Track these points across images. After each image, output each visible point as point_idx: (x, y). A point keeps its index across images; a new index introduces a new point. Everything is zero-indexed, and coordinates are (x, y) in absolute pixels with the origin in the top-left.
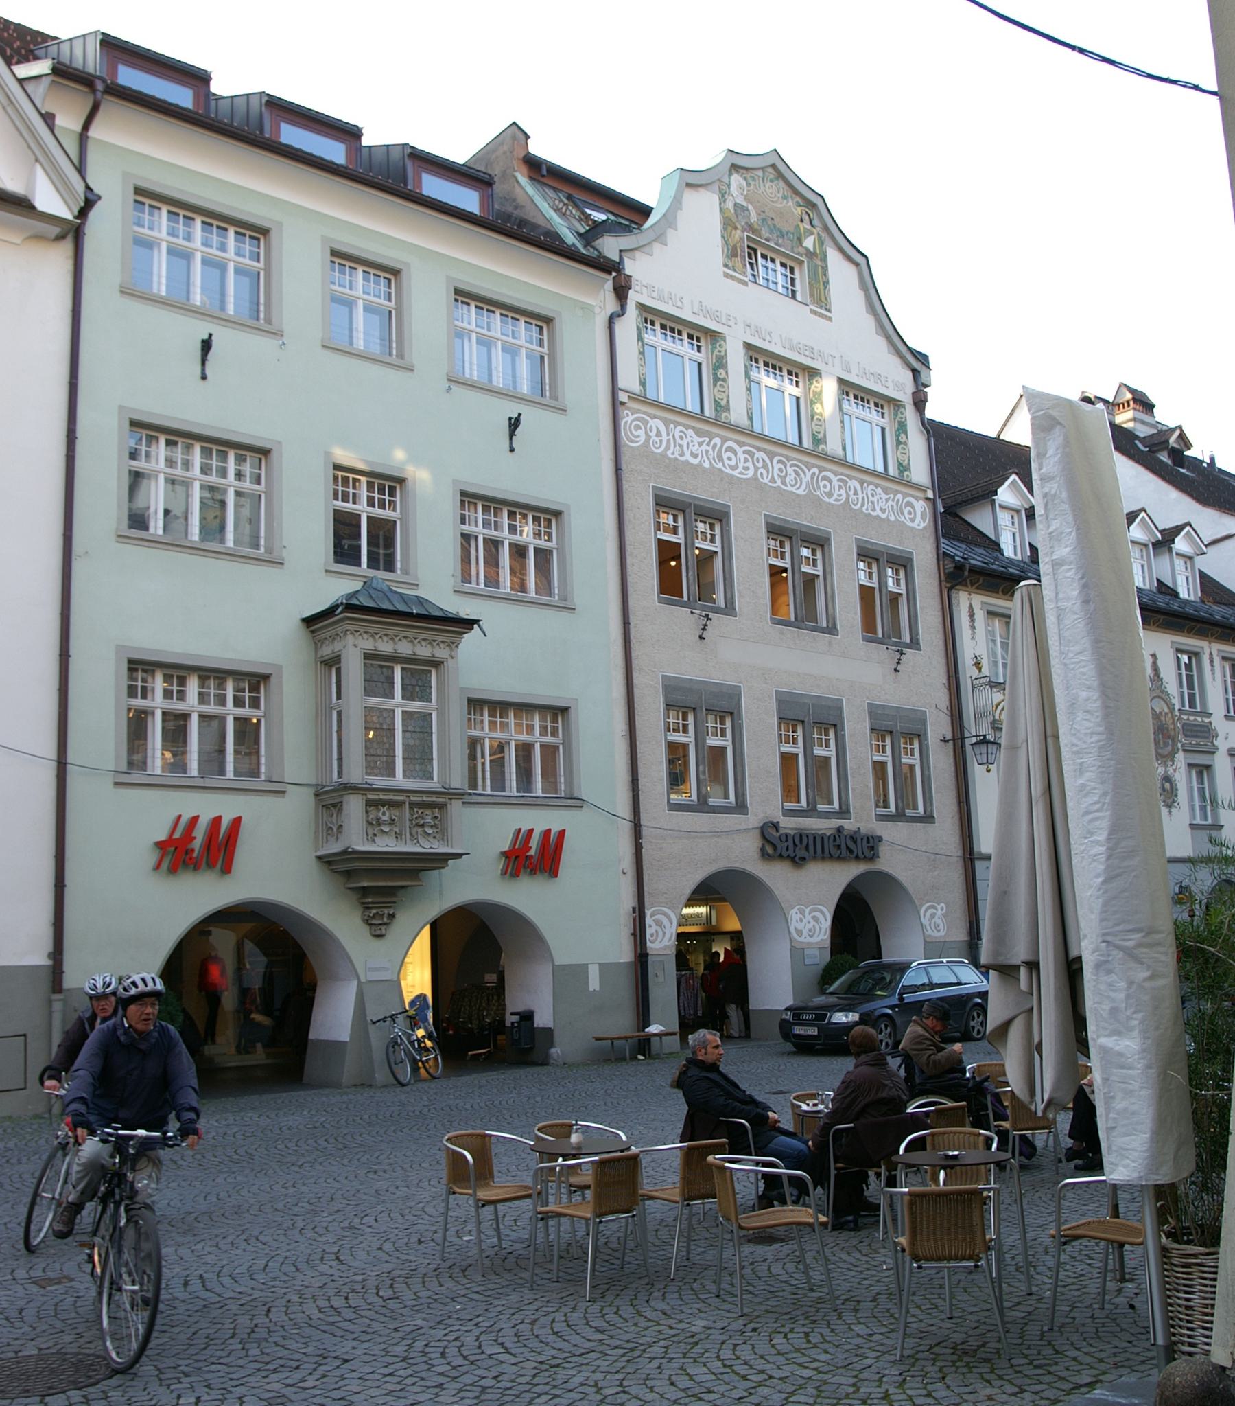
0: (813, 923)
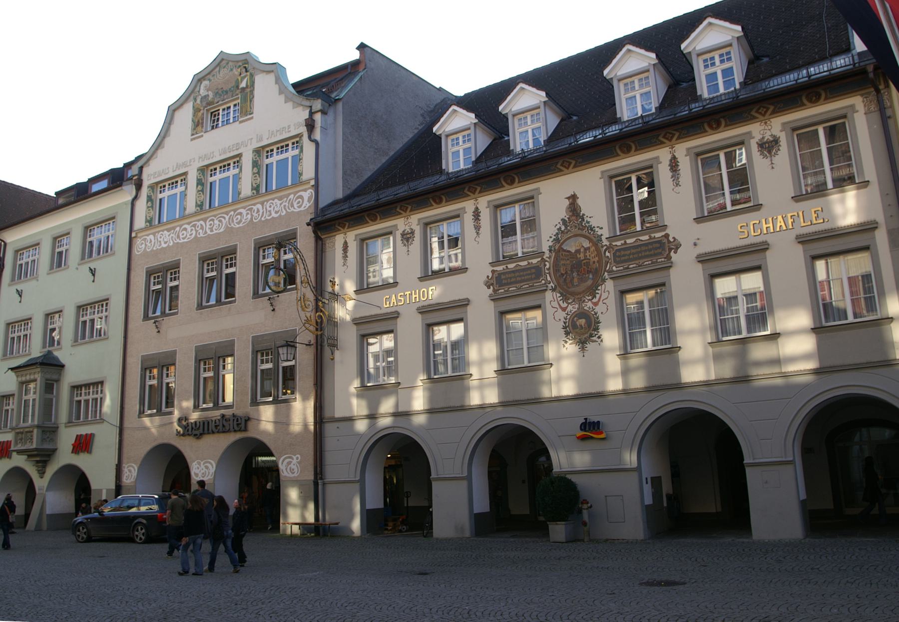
0: (205, 469)
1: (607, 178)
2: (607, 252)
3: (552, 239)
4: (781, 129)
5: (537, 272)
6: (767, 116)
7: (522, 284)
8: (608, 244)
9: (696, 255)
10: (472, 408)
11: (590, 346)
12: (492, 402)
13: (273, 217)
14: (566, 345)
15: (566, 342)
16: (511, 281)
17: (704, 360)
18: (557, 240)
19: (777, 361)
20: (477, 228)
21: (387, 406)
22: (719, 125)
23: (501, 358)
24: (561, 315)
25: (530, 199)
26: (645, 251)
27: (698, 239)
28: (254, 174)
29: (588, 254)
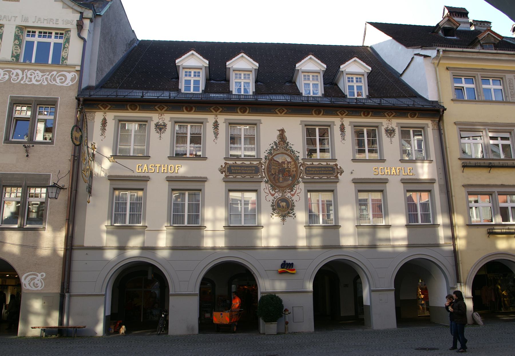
1: (117, 121)
2: (301, 167)
3: (267, 152)
4: (349, 124)
5: (256, 170)
6: (391, 117)
7: (246, 175)
8: (302, 162)
9: (352, 179)
10: (206, 249)
11: (288, 219)
12: (221, 246)
13: (33, 84)
14: (272, 216)
15: (273, 215)
16: (238, 172)
17: (353, 235)
18: (270, 153)
19: (388, 240)
20: (216, 134)
21: (136, 242)
22: (368, 114)
23: (228, 219)
24: (271, 198)
25: (254, 124)
26: (324, 171)
27: (353, 170)
28: (15, 44)
29: (289, 165)
